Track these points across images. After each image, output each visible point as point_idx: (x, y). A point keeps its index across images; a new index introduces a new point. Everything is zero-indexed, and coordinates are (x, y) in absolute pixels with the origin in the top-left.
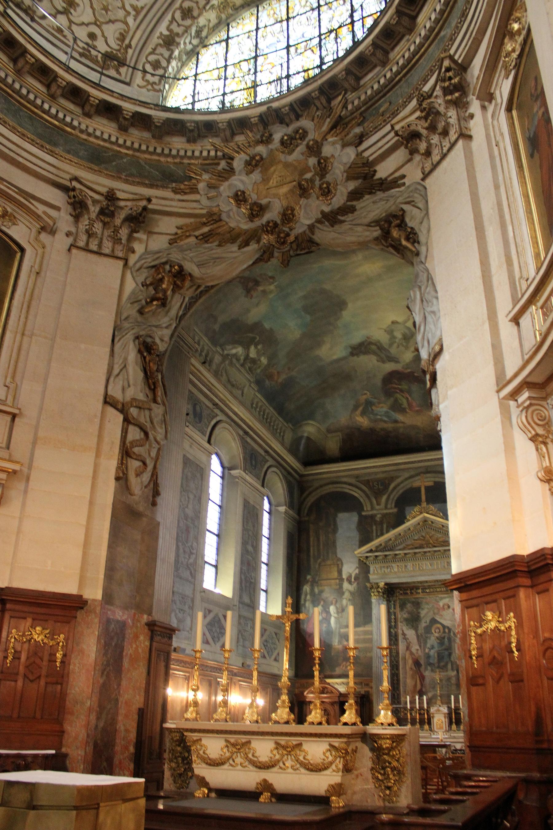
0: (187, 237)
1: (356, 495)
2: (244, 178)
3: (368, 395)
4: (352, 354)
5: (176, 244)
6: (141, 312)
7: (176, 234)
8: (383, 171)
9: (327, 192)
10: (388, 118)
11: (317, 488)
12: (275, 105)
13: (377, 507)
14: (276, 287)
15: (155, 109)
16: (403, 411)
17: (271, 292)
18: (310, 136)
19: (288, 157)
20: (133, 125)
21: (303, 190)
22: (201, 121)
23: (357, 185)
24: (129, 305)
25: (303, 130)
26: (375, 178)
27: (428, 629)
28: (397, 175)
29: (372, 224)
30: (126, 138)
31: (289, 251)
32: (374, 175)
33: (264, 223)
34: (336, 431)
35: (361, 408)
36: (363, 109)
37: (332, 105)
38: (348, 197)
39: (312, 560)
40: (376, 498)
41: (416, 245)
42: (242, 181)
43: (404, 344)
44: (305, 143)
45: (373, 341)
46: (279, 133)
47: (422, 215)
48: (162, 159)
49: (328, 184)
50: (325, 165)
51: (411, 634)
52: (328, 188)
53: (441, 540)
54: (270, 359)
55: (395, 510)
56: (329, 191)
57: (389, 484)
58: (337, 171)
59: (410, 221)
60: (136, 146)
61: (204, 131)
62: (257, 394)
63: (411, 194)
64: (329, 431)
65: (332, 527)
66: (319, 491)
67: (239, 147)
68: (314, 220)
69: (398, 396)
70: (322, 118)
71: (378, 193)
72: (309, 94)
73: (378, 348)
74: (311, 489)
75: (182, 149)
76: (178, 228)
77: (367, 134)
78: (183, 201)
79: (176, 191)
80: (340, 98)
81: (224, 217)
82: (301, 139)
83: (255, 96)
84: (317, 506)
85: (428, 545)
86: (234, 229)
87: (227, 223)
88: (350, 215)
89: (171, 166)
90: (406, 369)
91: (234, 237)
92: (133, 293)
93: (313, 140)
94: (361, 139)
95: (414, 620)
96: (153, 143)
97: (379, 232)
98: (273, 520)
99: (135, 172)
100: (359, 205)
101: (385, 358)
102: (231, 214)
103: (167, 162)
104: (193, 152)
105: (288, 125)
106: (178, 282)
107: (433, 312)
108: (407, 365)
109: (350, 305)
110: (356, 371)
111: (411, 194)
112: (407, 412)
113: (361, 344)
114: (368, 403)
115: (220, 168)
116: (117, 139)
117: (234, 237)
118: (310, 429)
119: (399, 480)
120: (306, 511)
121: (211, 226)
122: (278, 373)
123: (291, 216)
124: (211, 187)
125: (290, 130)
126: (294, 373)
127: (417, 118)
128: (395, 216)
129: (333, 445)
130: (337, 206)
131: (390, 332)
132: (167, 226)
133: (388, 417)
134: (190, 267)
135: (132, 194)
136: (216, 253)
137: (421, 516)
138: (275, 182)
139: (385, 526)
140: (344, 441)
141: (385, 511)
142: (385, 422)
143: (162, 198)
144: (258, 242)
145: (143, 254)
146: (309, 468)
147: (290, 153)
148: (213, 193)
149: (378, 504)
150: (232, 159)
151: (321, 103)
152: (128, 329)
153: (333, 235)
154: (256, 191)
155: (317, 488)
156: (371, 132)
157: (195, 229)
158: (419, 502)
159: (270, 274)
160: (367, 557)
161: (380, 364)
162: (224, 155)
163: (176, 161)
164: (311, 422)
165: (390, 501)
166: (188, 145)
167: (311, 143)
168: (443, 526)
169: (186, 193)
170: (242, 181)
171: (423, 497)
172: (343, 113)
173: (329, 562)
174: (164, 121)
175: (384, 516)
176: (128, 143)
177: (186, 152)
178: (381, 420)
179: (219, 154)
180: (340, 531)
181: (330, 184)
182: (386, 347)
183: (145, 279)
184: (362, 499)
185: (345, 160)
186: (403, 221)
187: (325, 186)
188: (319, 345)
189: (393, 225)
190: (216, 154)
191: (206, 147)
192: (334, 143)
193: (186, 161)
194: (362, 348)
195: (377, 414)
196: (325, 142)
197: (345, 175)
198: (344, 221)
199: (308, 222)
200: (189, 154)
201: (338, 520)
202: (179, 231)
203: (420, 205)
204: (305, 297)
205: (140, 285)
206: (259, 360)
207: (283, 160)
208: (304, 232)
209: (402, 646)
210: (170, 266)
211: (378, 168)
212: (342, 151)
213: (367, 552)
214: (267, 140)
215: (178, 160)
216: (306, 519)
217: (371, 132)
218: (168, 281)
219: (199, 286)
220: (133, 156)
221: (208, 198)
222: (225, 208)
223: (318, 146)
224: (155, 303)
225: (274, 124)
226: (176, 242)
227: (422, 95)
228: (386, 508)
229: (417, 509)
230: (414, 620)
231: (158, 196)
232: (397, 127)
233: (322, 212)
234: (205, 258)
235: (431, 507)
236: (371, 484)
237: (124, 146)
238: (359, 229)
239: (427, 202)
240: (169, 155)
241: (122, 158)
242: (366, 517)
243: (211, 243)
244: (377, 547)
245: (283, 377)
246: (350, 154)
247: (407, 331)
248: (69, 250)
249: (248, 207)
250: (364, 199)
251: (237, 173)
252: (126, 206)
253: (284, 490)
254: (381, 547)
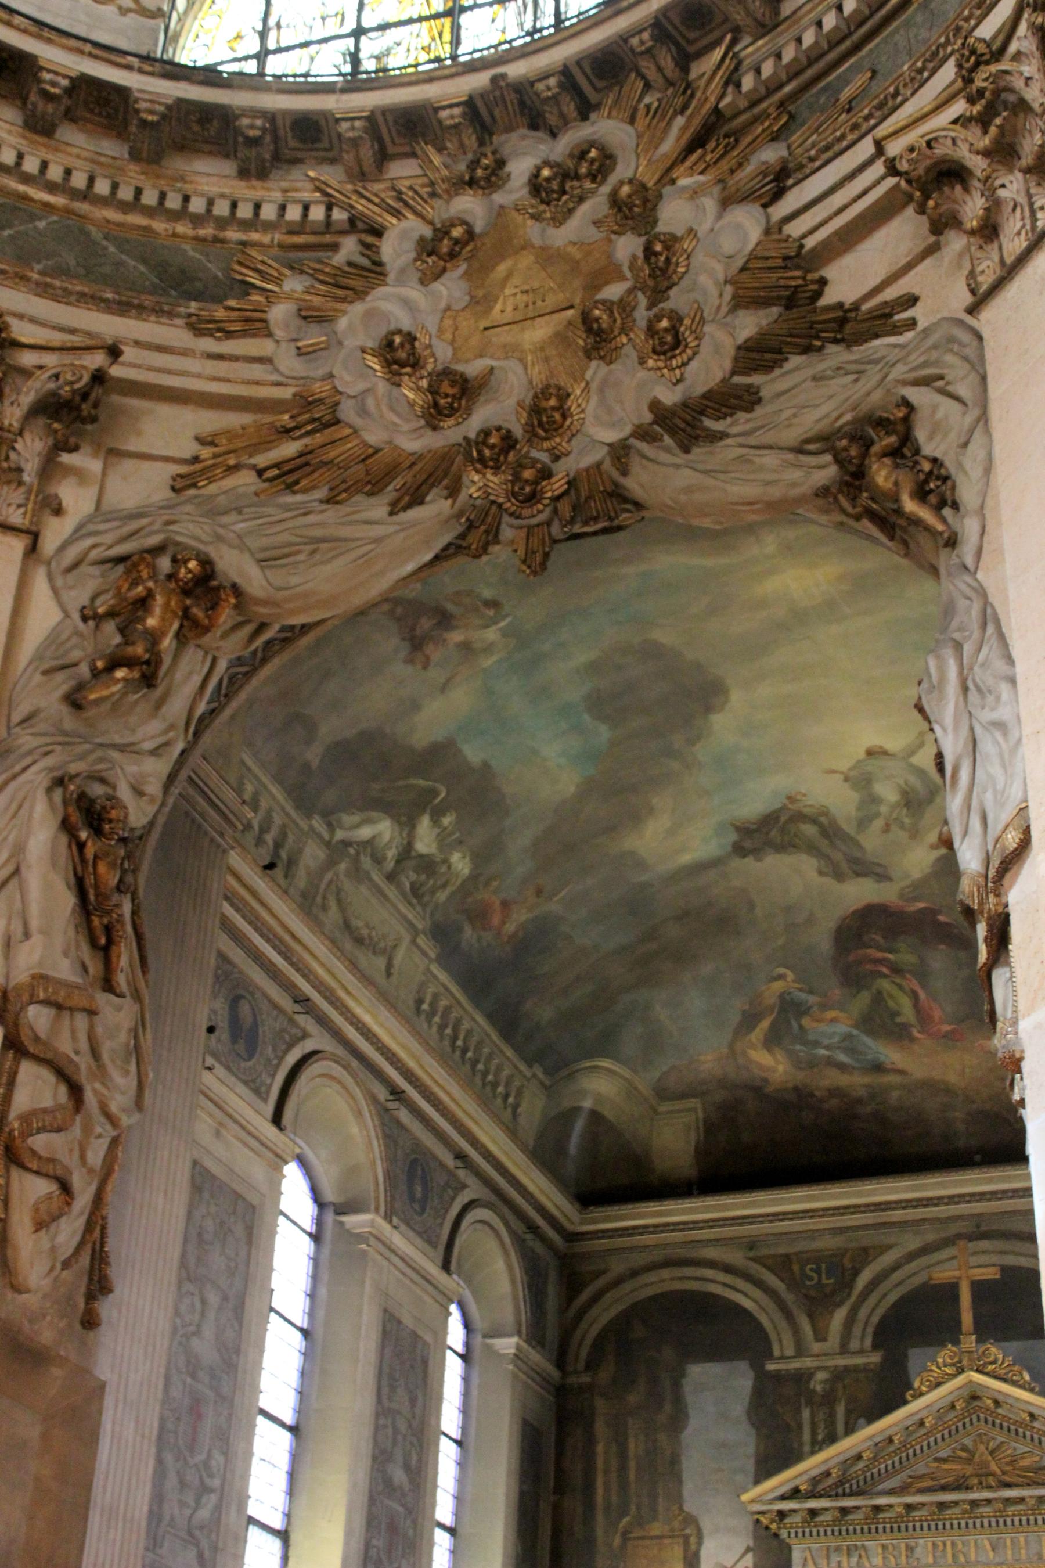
0: (232, 469)
1: (747, 1304)
2: (414, 293)
3: (787, 982)
4: (740, 850)
5: (192, 492)
6: (75, 701)
7: (196, 459)
8: (847, 281)
9: (670, 343)
10: (866, 118)
11: (619, 1281)
12: (516, 70)
13: (816, 1347)
14: (505, 633)
15: (141, 71)
16: (898, 1033)
17: (488, 649)
18: (623, 171)
19: (551, 231)
20: (70, 116)
21: (597, 338)
22: (286, 113)
23: (764, 322)
24: (38, 678)
25: (602, 149)
26: (823, 302)
28: (890, 294)
29: (811, 447)
30: (49, 157)
31: (549, 523)
32: (818, 294)
33: (472, 436)
34: (683, 1096)
35: (765, 1024)
36: (787, 89)
37: (693, 75)
38: (736, 359)
39: (600, 1517)
40: (811, 1316)
41: (947, 512)
42: (403, 301)
43: (907, 821)
44: (606, 189)
45: (806, 811)
46: (525, 157)
47: (969, 420)
48: (160, 226)
49: (676, 319)
50: (668, 260)
52: (674, 330)
53: (1025, 1463)
54: (480, 858)
55: (875, 1358)
56: (678, 342)
57: (856, 1273)
58: (704, 279)
59: (931, 438)
60: (79, 180)
61: (293, 143)
62: (435, 969)
63: (934, 355)
64: (662, 1093)
65: (668, 1408)
66: (628, 1286)
67: (399, 197)
68: (628, 430)
69: (885, 985)
70: (660, 115)
71: (831, 348)
72: (623, 39)
73: (824, 833)
74: (600, 1282)
75: (222, 196)
76: (201, 441)
77: (801, 167)
78: (220, 357)
79: (198, 327)
80: (717, 54)
81: (347, 411)
82: (593, 178)
83: (456, 41)
84: (618, 1338)
85: (984, 1478)
86: (377, 451)
87: (355, 432)
88: (741, 416)
89: (187, 247)
90: (915, 899)
91: (377, 476)
92: (53, 639)
93: (630, 181)
94: (780, 181)
96: (133, 176)
97: (833, 470)
98: (475, 1381)
99: (73, 263)
100: (766, 383)
101: (844, 866)
102: (370, 402)
103: (175, 235)
104: (257, 207)
105: (554, 135)
106: (198, 612)
107: (1000, 726)
108: (916, 886)
109: (736, 697)
110: (751, 906)
111: (934, 355)
112: (912, 1039)
113: (769, 820)
114: (790, 1009)
115: (339, 259)
116: (20, 156)
117: (377, 476)
118: (602, 1086)
119: (887, 1259)
120: (584, 1354)
121: (307, 440)
122: (505, 904)
123: (557, 416)
124: (309, 316)
125: (560, 148)
126: (554, 907)
127: (955, 122)
128: (882, 424)
129: (674, 1141)
130: (700, 390)
131: (860, 780)
133: (852, 1051)
134: (234, 565)
135: (62, 329)
136: (321, 524)
137: (961, 1380)
138: (509, 309)
139: (841, 1410)
140: (710, 1128)
141: (842, 1361)
142: (842, 1067)
143: (154, 345)
144: (453, 492)
145: (90, 519)
146: (597, 1212)
147: (558, 221)
148: (314, 337)
149: (820, 1336)
150: (378, 232)
151: (660, 69)
152: (30, 753)
153: (685, 477)
154: (448, 336)
155: (619, 1281)
156: (812, 160)
157: (256, 448)
158: (951, 1332)
159: (487, 593)
160: (782, 1515)
161: (829, 882)
162: (352, 221)
163: (202, 232)
164: (605, 1063)
165: (857, 1330)
166: (243, 184)
167: (626, 190)
168: (1032, 1415)
169: (229, 335)
170: (403, 301)
171: (967, 1319)
172: (727, 100)
173: (656, 1528)
174: (169, 107)
175: (839, 1375)
176: (55, 173)
177: (234, 205)
178: (831, 1062)
179: (338, 215)
180: (694, 1423)
181: (680, 320)
182: (850, 829)
183: (93, 599)
184: (767, 1317)
185: (728, 244)
186: (907, 438)
187: (665, 323)
188: (636, 818)
189: (875, 449)
190: (328, 216)
191: (296, 194)
192: (695, 193)
193: (233, 235)
194: (773, 831)
195: (816, 1044)
196: (667, 190)
197: (729, 290)
198: (722, 436)
199: (612, 436)
200: (245, 211)
201: (688, 1385)
202: (206, 452)
203: (963, 390)
204: (594, 668)
205: (76, 616)
206: (445, 861)
207: (537, 241)
208: (598, 465)
210: (174, 560)
211: (830, 272)
212: (719, 217)
213: (783, 1498)
214: (486, 177)
215: (207, 231)
216: (586, 1379)
217: (812, 160)
218: (167, 605)
219: (262, 627)
220: (68, 211)
221: (300, 352)
222: (349, 382)
223: (646, 201)
224: (120, 673)
225: (509, 129)
226: (194, 485)
227: (973, 52)
228: (844, 1349)
229: (945, 1355)
231: (142, 338)
232: (893, 149)
233: (655, 406)
234: (285, 537)
235: (994, 1351)
236: (796, 1268)
237: (39, 179)
238: (770, 460)
239: (984, 378)
240: (182, 214)
241: (32, 217)
242: (778, 1377)
243: (305, 491)
244: (815, 1481)
245: (520, 916)
247: (913, 780)
249: (424, 383)
250: (788, 366)
251: (391, 278)
252: (41, 367)
253: (513, 1282)
254: (830, 1481)
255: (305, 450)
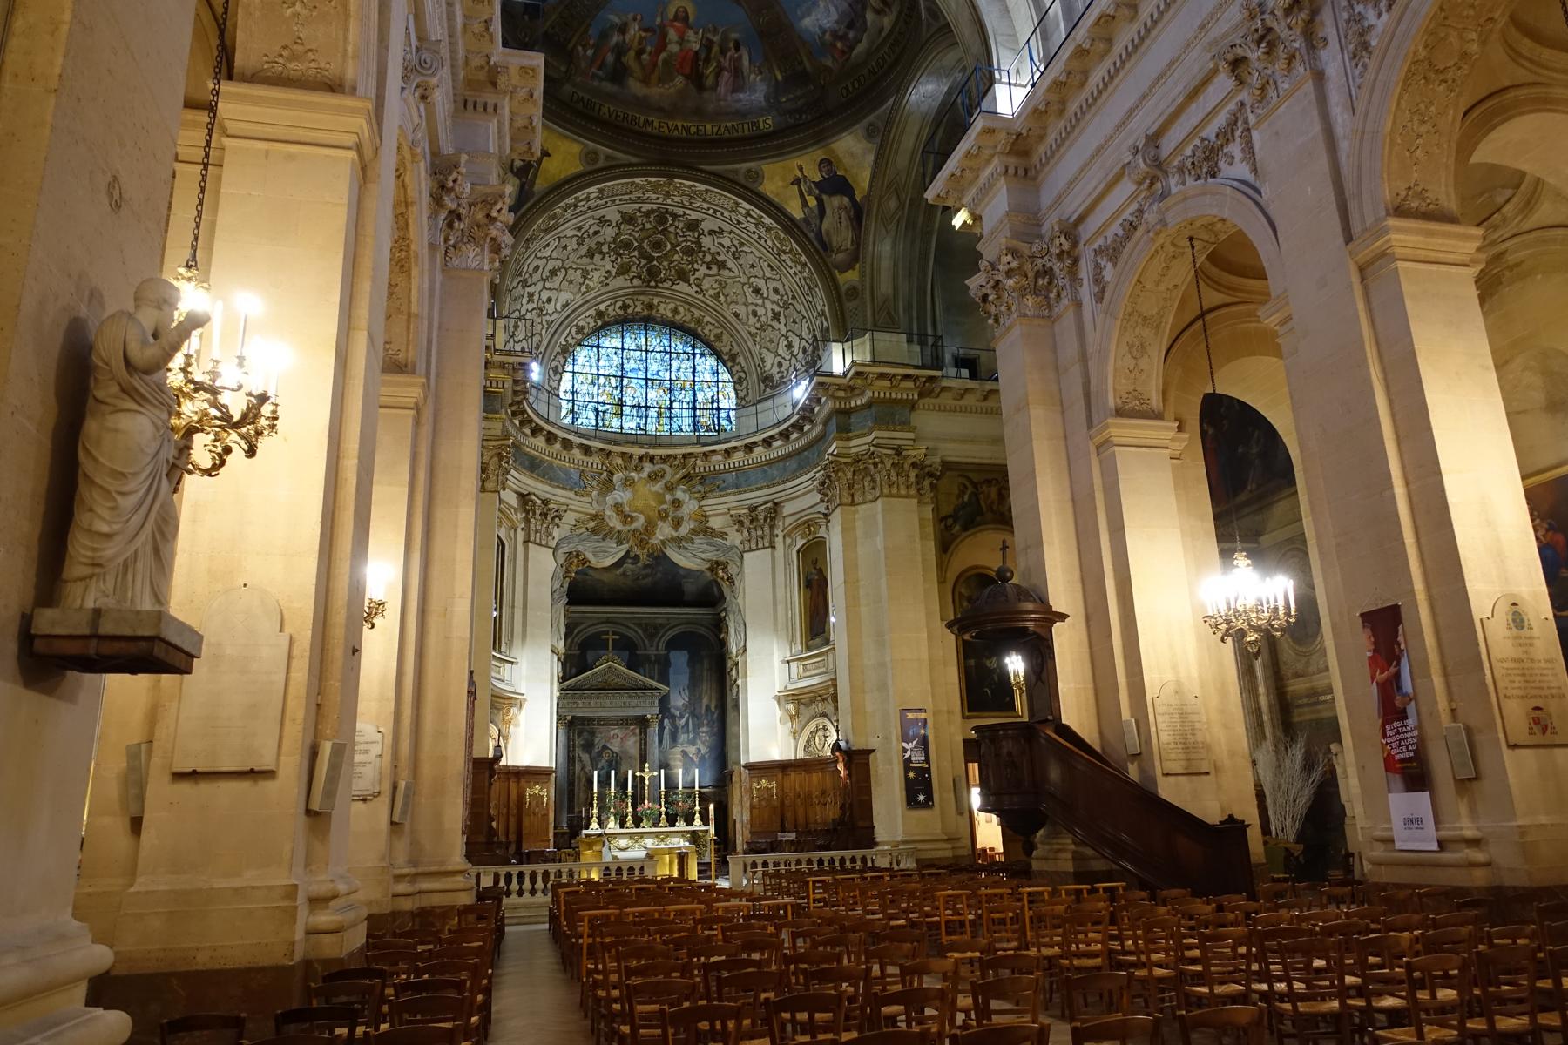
18: (668, 478)
21: (663, 516)
27: (600, 754)
42: (620, 495)
51: (585, 757)
95: (588, 747)
132: (570, 518)
134: (590, 556)
209: (578, 767)
222: (608, 512)
230: (588, 747)
246: (695, 502)
248: (526, 542)
255: (599, 528)
